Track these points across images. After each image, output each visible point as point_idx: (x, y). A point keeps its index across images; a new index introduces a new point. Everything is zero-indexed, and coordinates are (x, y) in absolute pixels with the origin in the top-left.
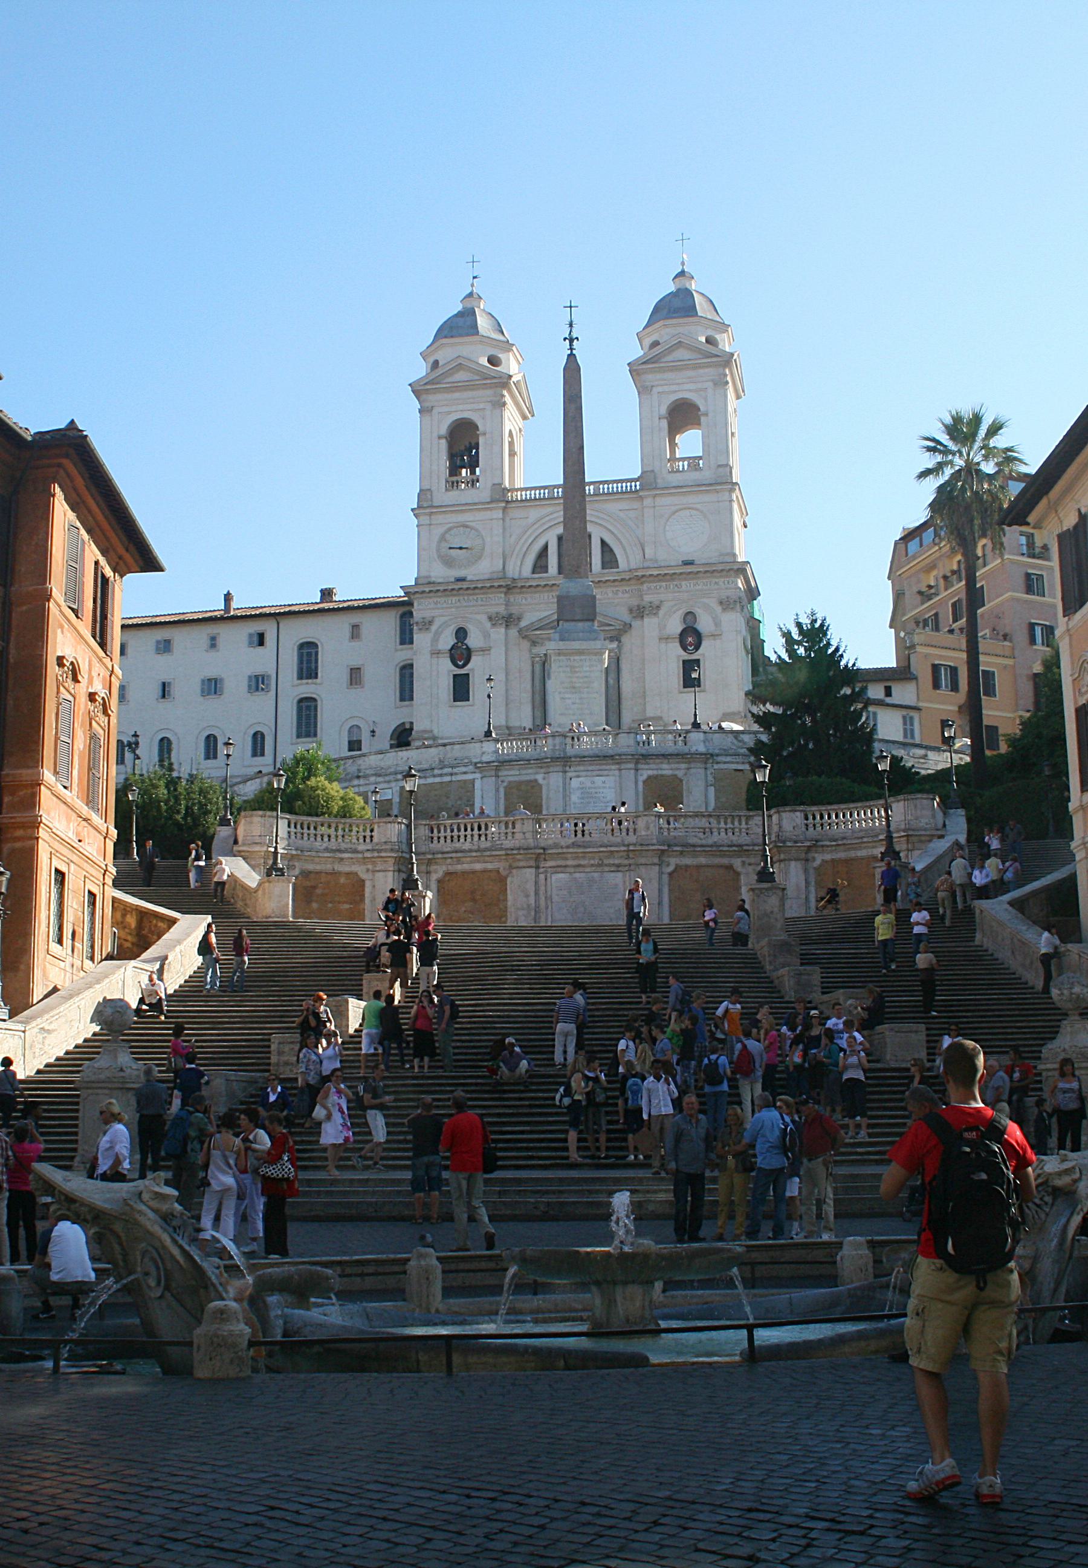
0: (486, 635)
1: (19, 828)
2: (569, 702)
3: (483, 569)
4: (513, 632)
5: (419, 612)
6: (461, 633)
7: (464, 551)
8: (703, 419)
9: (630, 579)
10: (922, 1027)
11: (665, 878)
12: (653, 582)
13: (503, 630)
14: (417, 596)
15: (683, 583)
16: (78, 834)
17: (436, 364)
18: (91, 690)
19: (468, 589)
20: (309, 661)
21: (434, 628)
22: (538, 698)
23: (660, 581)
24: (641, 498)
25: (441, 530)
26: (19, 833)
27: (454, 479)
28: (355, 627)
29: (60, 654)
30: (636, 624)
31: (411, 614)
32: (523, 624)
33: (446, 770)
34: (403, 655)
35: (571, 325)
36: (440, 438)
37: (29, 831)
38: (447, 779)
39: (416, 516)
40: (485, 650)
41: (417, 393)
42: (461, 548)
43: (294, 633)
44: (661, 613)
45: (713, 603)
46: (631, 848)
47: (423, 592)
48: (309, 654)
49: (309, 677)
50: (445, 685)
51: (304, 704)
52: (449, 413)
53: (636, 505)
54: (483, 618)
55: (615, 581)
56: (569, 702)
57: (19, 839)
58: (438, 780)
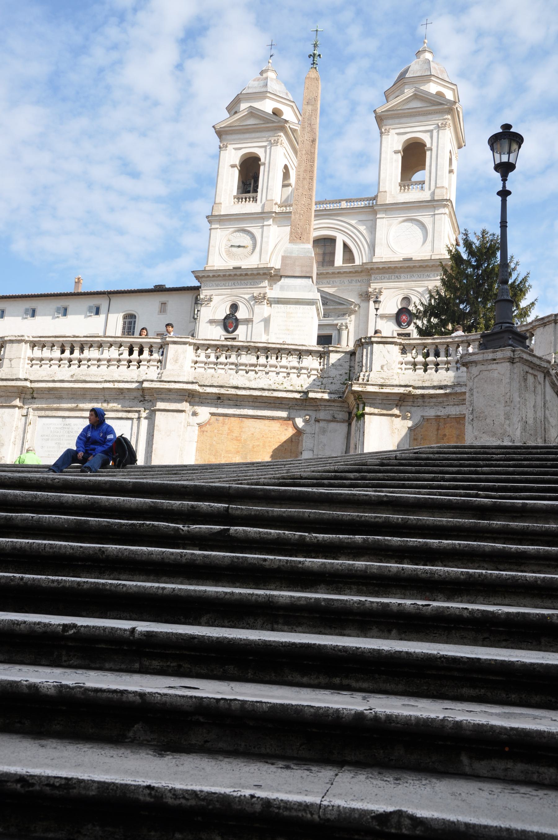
6: (234, 307)
7: (240, 249)
8: (428, 153)
9: (361, 272)
12: (379, 273)
14: (204, 279)
15: (402, 275)
19: (241, 275)
23: (387, 273)
24: (375, 213)
28: (164, 304)
30: (363, 305)
31: (199, 295)
36: (233, 166)
39: (210, 222)
40: (248, 321)
42: (239, 247)
47: (208, 276)
52: (240, 149)
53: (371, 217)
55: (350, 272)
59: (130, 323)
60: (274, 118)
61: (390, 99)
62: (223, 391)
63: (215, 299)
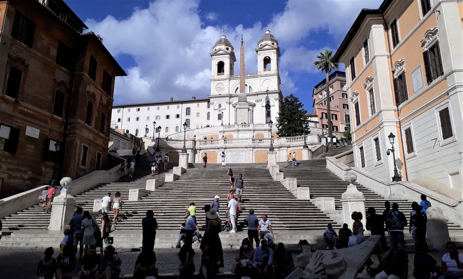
0: (225, 106)
1: (71, 134)
2: (240, 119)
3: (225, 92)
4: (231, 105)
5: (212, 100)
6: (220, 106)
8: (271, 60)
10: (308, 188)
11: (254, 153)
13: (229, 105)
16: (94, 138)
17: (215, 50)
18: (101, 102)
20: (188, 112)
21: (214, 105)
22: (236, 119)
25: (216, 84)
26: (71, 136)
27: (219, 73)
29: (88, 89)
31: (210, 102)
32: (233, 104)
33: (212, 133)
34: (208, 110)
35: (242, 39)
37: (74, 135)
38: (213, 134)
41: (211, 55)
43: (185, 106)
44: (262, 101)
45: (273, 99)
46: (246, 146)
48: (188, 110)
49: (188, 115)
50: (217, 117)
51: (187, 121)
54: (225, 102)
56: (240, 119)
57: (71, 137)
58: (211, 135)
59: (188, 110)
60: (227, 51)
61: (260, 45)
62: (258, 147)
63: (215, 103)
